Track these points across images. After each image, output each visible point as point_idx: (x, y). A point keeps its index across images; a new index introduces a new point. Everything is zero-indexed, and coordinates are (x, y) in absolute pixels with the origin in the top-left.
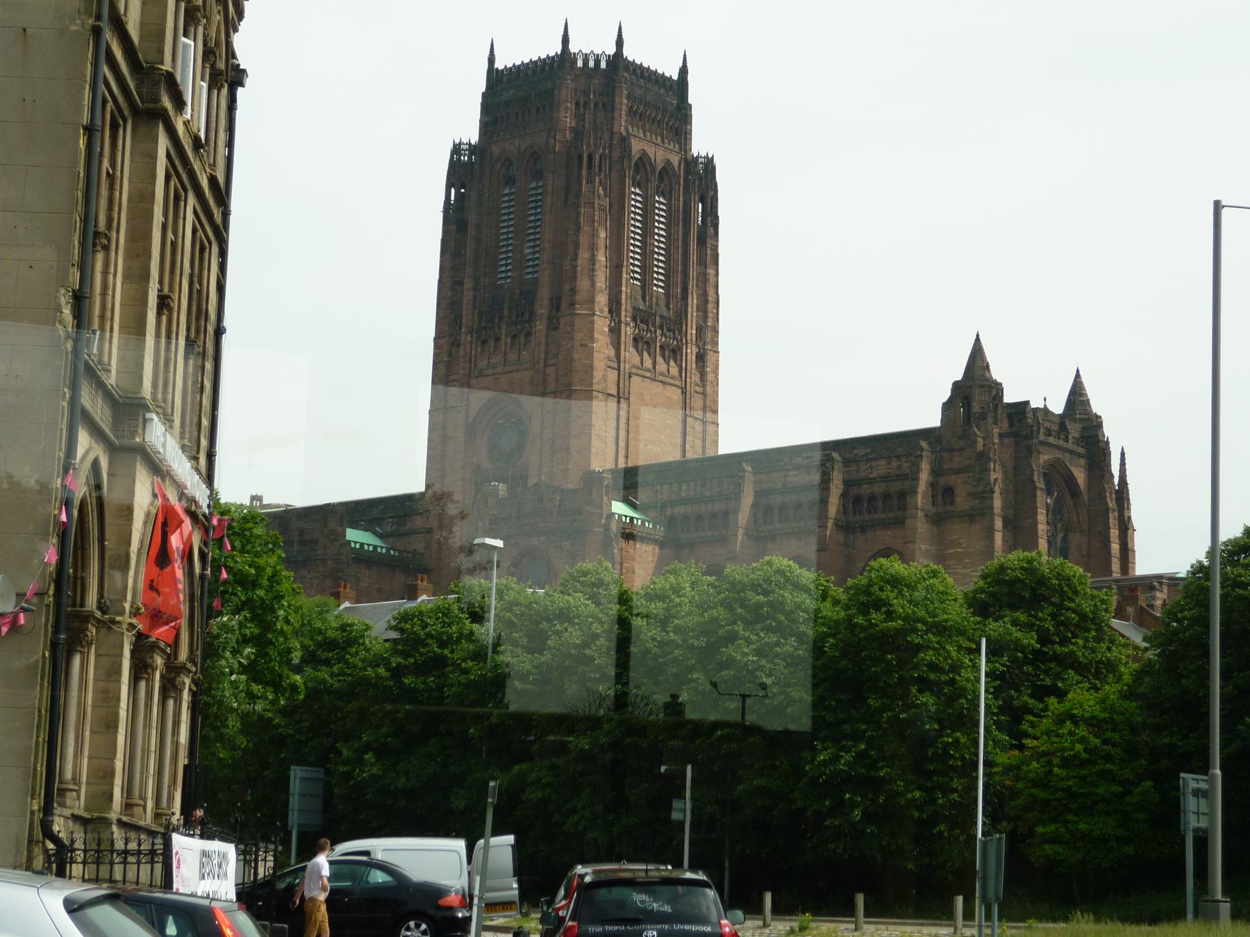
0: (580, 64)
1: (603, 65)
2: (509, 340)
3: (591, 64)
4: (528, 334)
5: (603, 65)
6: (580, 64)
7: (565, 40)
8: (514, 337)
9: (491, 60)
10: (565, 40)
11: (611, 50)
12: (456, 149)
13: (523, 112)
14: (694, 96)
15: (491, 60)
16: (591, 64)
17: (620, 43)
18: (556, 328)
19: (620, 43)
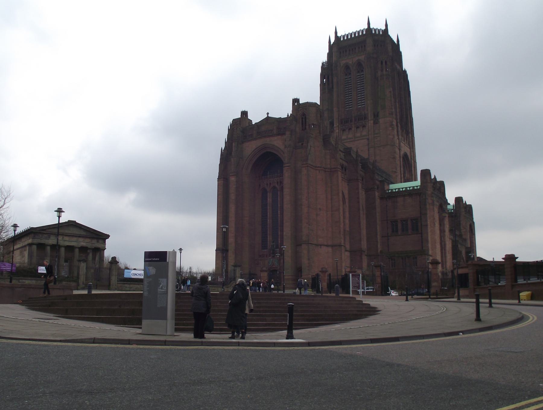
0: (373, 32)
1: (381, 33)
2: (355, 128)
3: (377, 32)
4: (364, 126)
5: (381, 33)
6: (373, 32)
8: (358, 127)
9: (336, 33)
12: (323, 64)
13: (352, 49)
14: (401, 49)
15: (336, 33)
16: (377, 32)
17: (386, 25)
18: (377, 123)
19: (386, 25)
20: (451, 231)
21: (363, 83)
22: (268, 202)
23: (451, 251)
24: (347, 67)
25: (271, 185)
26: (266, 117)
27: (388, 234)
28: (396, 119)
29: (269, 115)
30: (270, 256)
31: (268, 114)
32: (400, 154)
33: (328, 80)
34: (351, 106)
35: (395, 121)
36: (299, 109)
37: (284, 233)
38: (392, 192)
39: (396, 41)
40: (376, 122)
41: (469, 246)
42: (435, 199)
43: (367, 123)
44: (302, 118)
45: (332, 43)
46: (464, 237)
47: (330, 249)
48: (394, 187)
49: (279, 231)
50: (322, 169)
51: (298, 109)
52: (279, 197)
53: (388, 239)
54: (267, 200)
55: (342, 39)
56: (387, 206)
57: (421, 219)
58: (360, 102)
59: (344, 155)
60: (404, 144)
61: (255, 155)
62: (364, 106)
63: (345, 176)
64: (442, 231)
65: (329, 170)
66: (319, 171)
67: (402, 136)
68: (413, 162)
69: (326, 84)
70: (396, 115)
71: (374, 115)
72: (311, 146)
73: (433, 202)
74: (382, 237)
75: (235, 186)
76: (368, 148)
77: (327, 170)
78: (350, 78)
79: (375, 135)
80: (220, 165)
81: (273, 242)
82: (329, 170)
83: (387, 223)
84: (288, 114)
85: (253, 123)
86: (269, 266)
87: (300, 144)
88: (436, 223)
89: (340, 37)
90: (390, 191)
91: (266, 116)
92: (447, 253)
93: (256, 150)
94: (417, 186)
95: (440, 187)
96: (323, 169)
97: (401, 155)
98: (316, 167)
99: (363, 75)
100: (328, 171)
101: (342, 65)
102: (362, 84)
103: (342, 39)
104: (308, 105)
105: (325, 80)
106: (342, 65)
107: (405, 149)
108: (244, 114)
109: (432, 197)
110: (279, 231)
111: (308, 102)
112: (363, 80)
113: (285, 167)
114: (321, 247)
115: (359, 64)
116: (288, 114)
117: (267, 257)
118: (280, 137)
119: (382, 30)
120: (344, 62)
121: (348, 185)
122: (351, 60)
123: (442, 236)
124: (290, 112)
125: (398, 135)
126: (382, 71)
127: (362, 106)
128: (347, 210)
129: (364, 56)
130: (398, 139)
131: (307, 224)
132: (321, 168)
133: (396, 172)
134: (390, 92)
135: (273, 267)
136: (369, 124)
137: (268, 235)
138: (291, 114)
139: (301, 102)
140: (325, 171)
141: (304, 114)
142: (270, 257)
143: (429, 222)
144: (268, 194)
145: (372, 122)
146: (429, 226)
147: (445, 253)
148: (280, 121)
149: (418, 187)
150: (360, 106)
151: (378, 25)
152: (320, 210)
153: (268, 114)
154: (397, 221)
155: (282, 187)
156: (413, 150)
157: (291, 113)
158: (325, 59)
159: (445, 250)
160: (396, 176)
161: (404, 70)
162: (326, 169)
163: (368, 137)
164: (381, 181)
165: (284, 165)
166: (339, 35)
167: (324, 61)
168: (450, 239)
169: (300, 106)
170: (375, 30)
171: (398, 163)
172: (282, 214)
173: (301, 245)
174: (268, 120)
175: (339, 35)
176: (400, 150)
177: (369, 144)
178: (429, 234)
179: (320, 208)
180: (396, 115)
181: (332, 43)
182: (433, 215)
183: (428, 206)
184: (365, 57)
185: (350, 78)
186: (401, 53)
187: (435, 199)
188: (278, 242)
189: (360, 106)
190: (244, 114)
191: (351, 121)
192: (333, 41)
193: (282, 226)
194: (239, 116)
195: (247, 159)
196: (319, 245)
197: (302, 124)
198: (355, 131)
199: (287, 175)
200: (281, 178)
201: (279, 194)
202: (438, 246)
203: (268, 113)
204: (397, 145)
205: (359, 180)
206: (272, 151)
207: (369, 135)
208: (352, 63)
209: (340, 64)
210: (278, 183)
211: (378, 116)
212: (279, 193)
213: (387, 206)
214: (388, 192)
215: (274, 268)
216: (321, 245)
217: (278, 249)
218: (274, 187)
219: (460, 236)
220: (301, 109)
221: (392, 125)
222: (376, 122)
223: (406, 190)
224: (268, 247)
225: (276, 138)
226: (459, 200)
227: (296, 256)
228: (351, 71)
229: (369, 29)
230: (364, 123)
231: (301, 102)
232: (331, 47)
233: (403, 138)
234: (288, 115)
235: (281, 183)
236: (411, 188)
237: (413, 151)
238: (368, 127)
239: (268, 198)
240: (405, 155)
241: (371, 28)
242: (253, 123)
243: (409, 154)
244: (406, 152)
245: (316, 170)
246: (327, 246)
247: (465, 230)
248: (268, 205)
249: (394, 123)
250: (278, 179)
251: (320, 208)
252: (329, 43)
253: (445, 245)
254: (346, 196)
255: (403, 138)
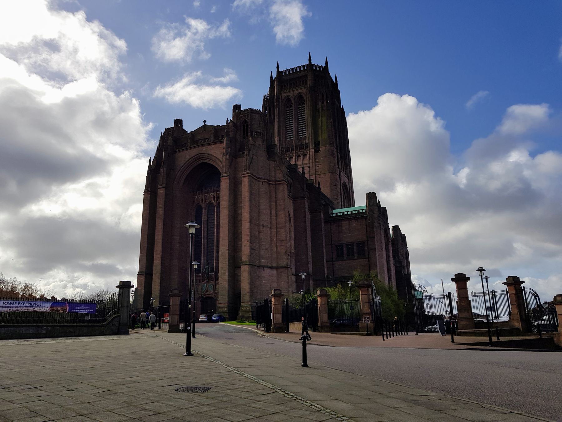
0: (314, 68)
1: (321, 70)
2: (296, 157)
3: (318, 69)
4: (305, 155)
5: (321, 70)
6: (314, 68)
7: (310, 60)
8: (299, 156)
9: (278, 68)
10: (310, 60)
11: (324, 65)
12: (264, 97)
15: (278, 68)
16: (318, 69)
17: (327, 63)
19: (327, 63)
20: (394, 257)
21: (305, 114)
22: (203, 219)
23: (395, 277)
24: (288, 100)
25: (207, 200)
26: (203, 125)
27: (333, 259)
28: (337, 149)
29: (206, 123)
30: (204, 281)
31: (205, 121)
32: (340, 182)
33: (269, 112)
34: (292, 136)
35: (336, 150)
36: (241, 116)
37: (220, 253)
38: (336, 216)
39: (334, 80)
40: (317, 151)
41: (407, 273)
42: (381, 223)
43: (308, 152)
44: (244, 126)
45: (274, 79)
46: (403, 264)
47: (275, 272)
48: (339, 211)
49: (215, 251)
50: (265, 181)
51: (239, 115)
52: (215, 213)
53: (333, 264)
54: (202, 217)
55: (284, 74)
56: (331, 230)
57: (368, 243)
58: (301, 132)
59: (289, 172)
60: (344, 174)
61: (189, 166)
62: (305, 136)
63: (290, 193)
64: (388, 256)
65: (274, 183)
66: (262, 183)
67: (342, 167)
68: (351, 192)
69: (268, 115)
70: (337, 145)
71: (315, 146)
72: (253, 154)
73: (380, 226)
74: (327, 262)
75: (164, 200)
76: (310, 176)
77: (271, 183)
78: (291, 110)
79: (316, 164)
80: (148, 177)
81: (208, 265)
82: (274, 183)
83: (332, 247)
84: (227, 119)
85: (188, 132)
86: (202, 293)
87: (241, 153)
88: (383, 247)
89: (282, 72)
90: (334, 215)
91: (203, 124)
92: (393, 278)
93: (190, 161)
94: (363, 210)
95: (383, 212)
96: (267, 181)
97: (342, 184)
98: (259, 178)
99: (304, 107)
100: (272, 184)
101: (283, 97)
102: (303, 115)
103: (284, 74)
104: (251, 111)
105: (266, 112)
106: (283, 97)
107: (345, 179)
108: (178, 122)
109: (379, 220)
110: (215, 251)
111: (250, 108)
112: (304, 112)
113: (222, 177)
114: (264, 270)
115: (300, 98)
116: (227, 119)
117: (200, 282)
118: (217, 145)
119: (323, 67)
120: (285, 94)
121: (293, 203)
122: (292, 93)
123: (388, 262)
124: (230, 118)
125: (338, 164)
126: (323, 103)
127: (304, 136)
128: (293, 229)
129: (305, 89)
130: (339, 168)
131: (247, 242)
132: (264, 179)
133: (338, 199)
134: (331, 122)
135: (207, 293)
136: (311, 153)
137: (202, 257)
138: (231, 120)
139: (242, 109)
140: (269, 184)
141: (245, 122)
142: (204, 282)
143: (376, 246)
144: (203, 210)
145: (313, 150)
146: (377, 250)
147: (391, 279)
148: (217, 129)
149: (364, 211)
150: (301, 137)
151: (318, 61)
152: (263, 227)
153: (205, 121)
154: (343, 245)
155: (219, 203)
156: (351, 180)
157: (232, 119)
158: (267, 92)
159: (391, 275)
160: (338, 203)
161: (342, 107)
162: (270, 182)
163: (309, 165)
164: (324, 205)
165: (221, 175)
166: (281, 70)
167: (266, 94)
168: (393, 264)
169: (241, 113)
170: (316, 66)
171: (339, 190)
172: (218, 233)
173: (241, 267)
174: (205, 128)
175: (281, 70)
176: (340, 178)
177: (310, 172)
178: (377, 258)
179: (263, 225)
180: (337, 145)
181: (274, 79)
182: (380, 238)
183: (375, 230)
184: (306, 90)
185: (291, 110)
186: (339, 91)
187: (381, 223)
188: (214, 265)
189: (301, 137)
190: (178, 122)
191: (292, 150)
192: (274, 76)
193: (218, 246)
194: (172, 125)
195: (179, 171)
196: (262, 267)
197: (244, 132)
198: (297, 160)
199: (225, 184)
200: (218, 192)
201: (215, 211)
202: (386, 271)
203: (205, 120)
204: (338, 174)
205: (305, 198)
206: (208, 162)
207: (310, 163)
208: (294, 95)
209: (282, 96)
210: (214, 198)
211: (319, 145)
212: (215, 208)
213: (331, 230)
214: (332, 215)
215: (208, 294)
216: (264, 267)
217: (213, 273)
218: (211, 203)
219: (400, 262)
220: (242, 115)
221: (334, 153)
222: (317, 151)
223: (351, 214)
224: (202, 271)
225: (213, 146)
226: (396, 229)
227: (234, 279)
228: (292, 104)
229: (310, 65)
230: (305, 152)
231: (242, 109)
232: (272, 82)
233: (342, 169)
234: (227, 121)
235: (218, 198)
236: (356, 212)
237: (351, 182)
238: (309, 155)
239: (203, 215)
240: (345, 185)
241: (312, 64)
242: (188, 132)
243: (347, 184)
244: (345, 181)
245: (259, 181)
246: (271, 268)
247: (403, 257)
248: (203, 222)
249: (335, 152)
250: (215, 194)
251: (263, 225)
252: (271, 78)
253: (390, 270)
254: (292, 215)
255: (342, 169)
